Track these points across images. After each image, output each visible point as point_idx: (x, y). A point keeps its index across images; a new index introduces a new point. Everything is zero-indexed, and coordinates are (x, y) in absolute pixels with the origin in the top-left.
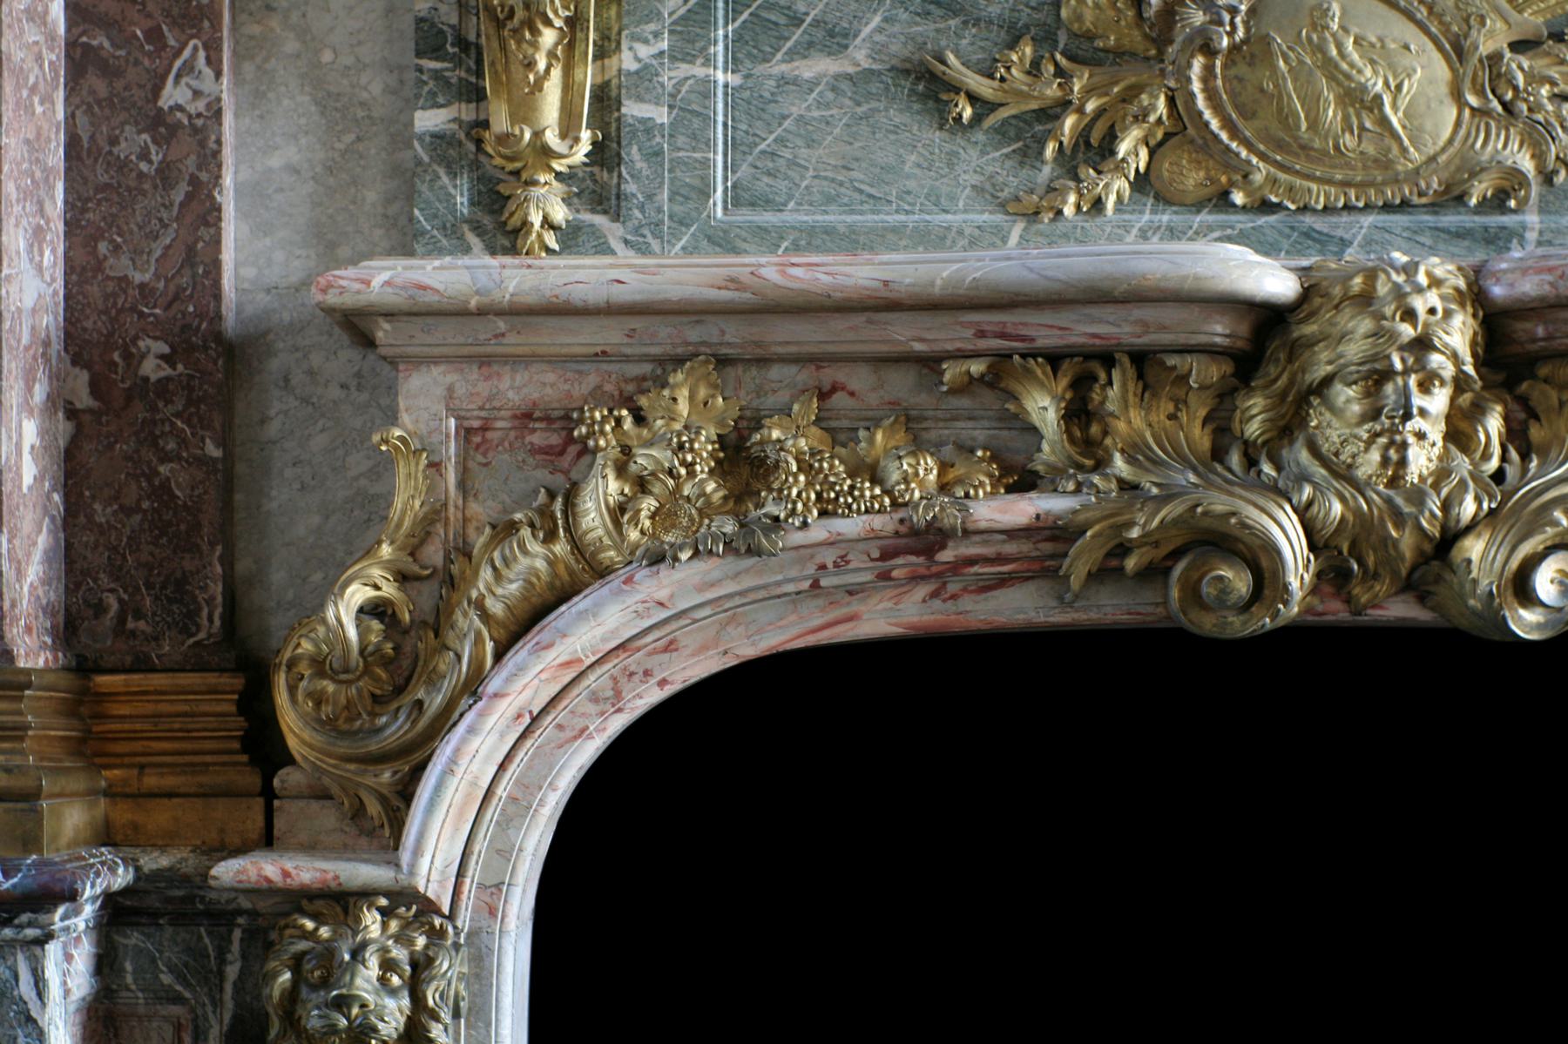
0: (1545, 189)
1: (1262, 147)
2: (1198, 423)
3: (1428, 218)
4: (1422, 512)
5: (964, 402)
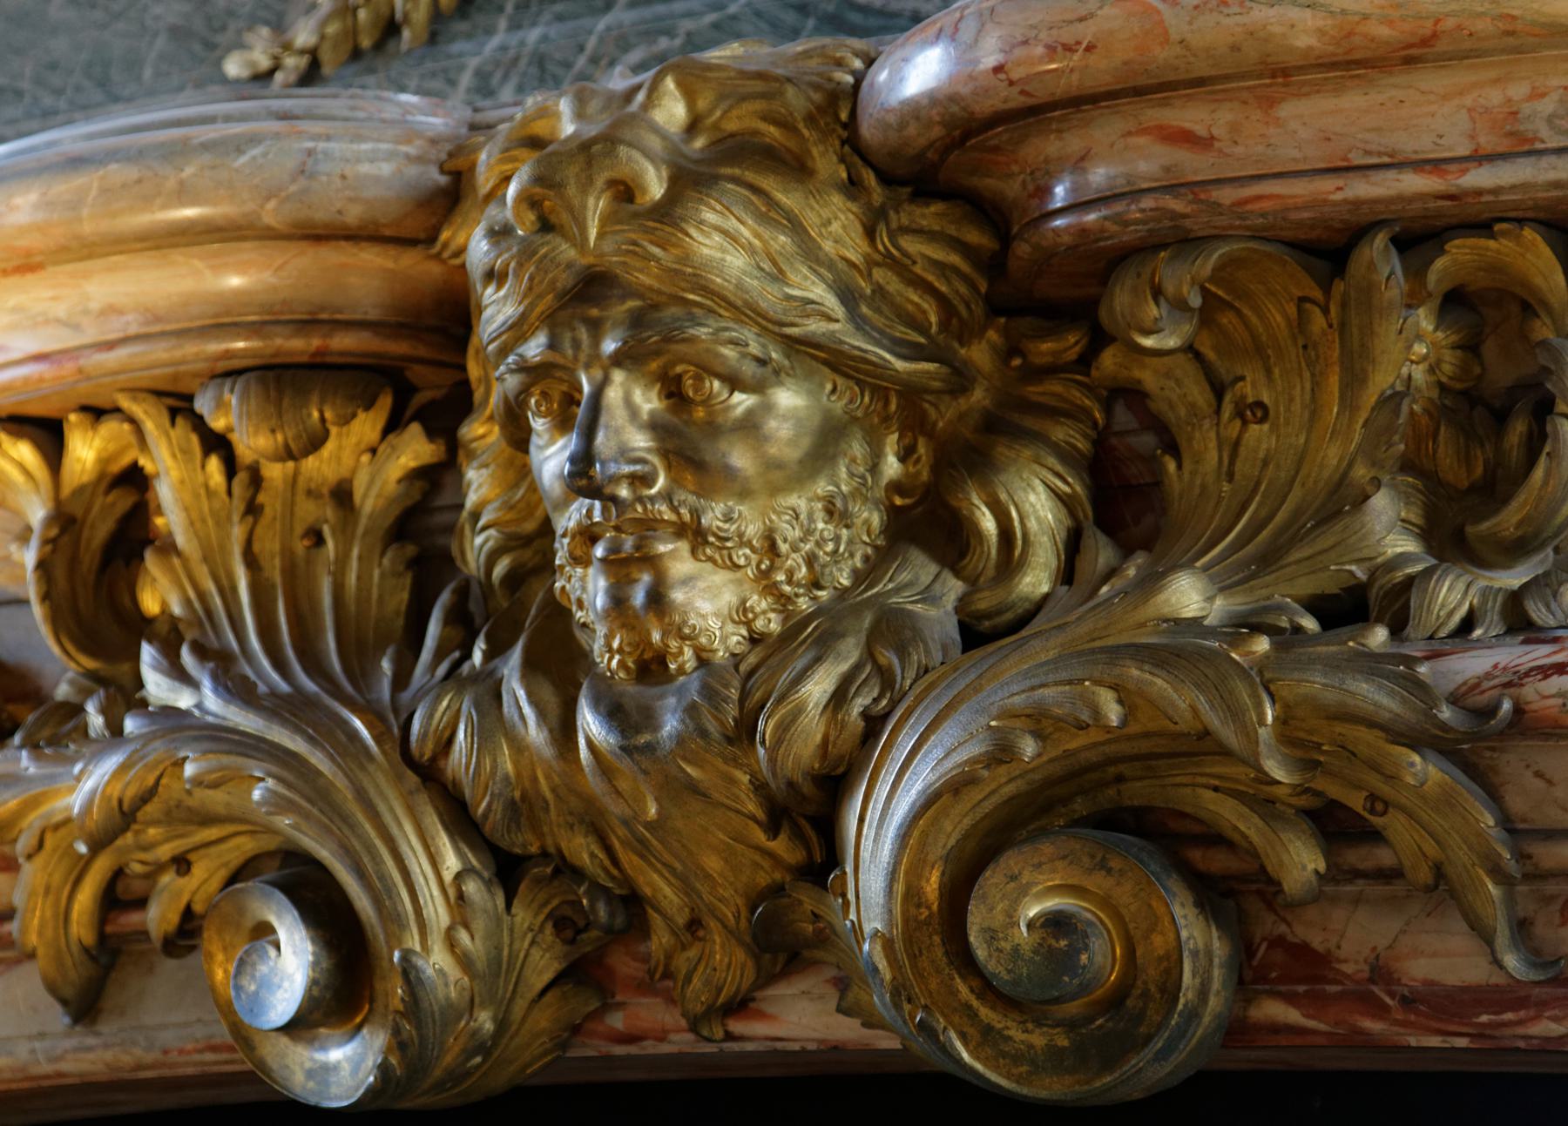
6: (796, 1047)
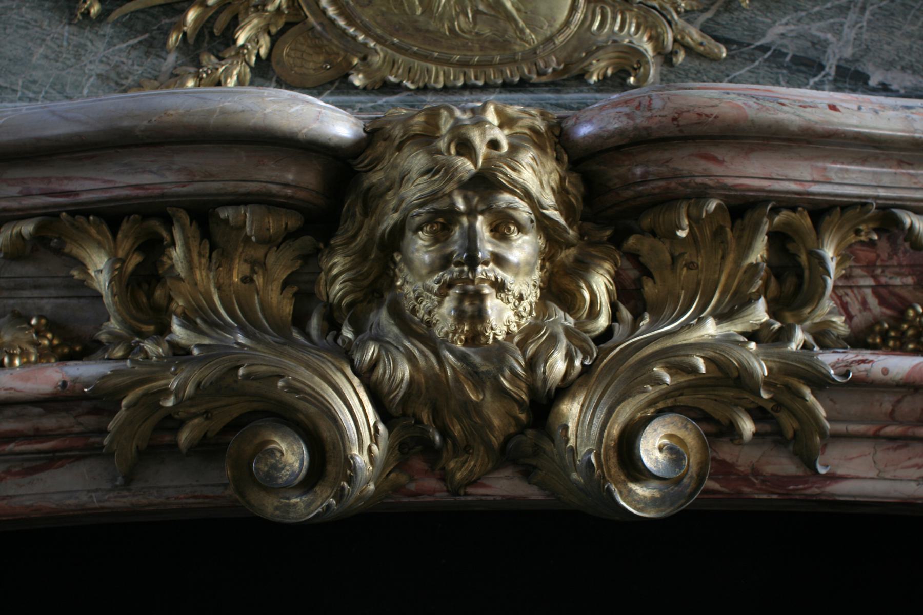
0: (665, 69)
1: (379, 31)
2: (276, 286)
3: (551, 96)
4: (501, 371)
5: (27, 270)
6: (492, 498)
